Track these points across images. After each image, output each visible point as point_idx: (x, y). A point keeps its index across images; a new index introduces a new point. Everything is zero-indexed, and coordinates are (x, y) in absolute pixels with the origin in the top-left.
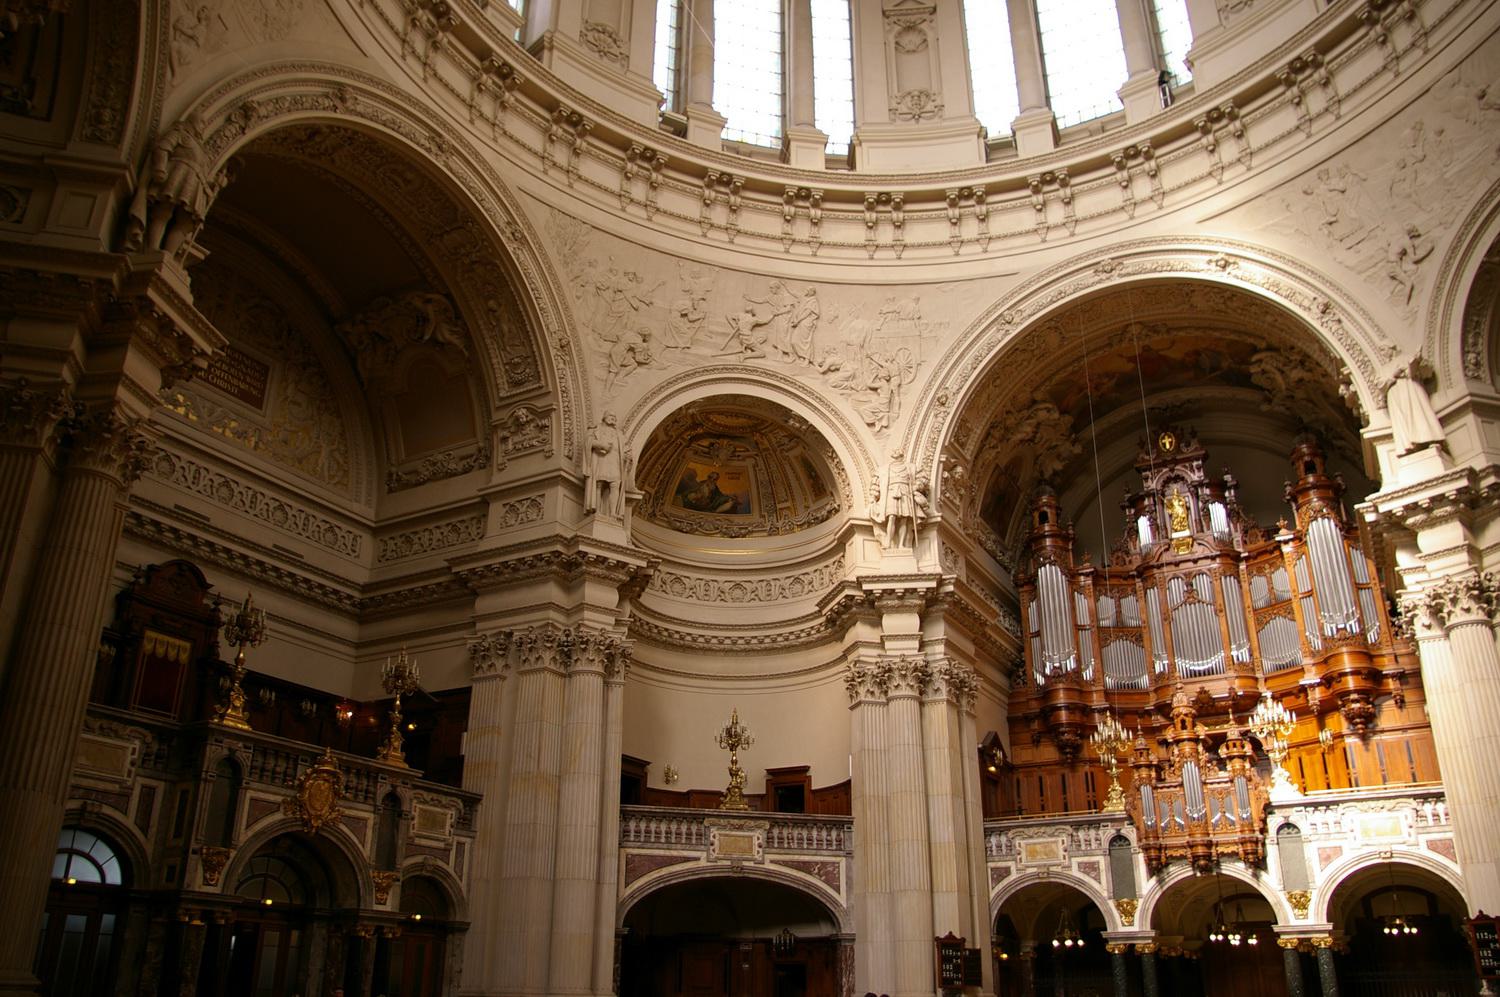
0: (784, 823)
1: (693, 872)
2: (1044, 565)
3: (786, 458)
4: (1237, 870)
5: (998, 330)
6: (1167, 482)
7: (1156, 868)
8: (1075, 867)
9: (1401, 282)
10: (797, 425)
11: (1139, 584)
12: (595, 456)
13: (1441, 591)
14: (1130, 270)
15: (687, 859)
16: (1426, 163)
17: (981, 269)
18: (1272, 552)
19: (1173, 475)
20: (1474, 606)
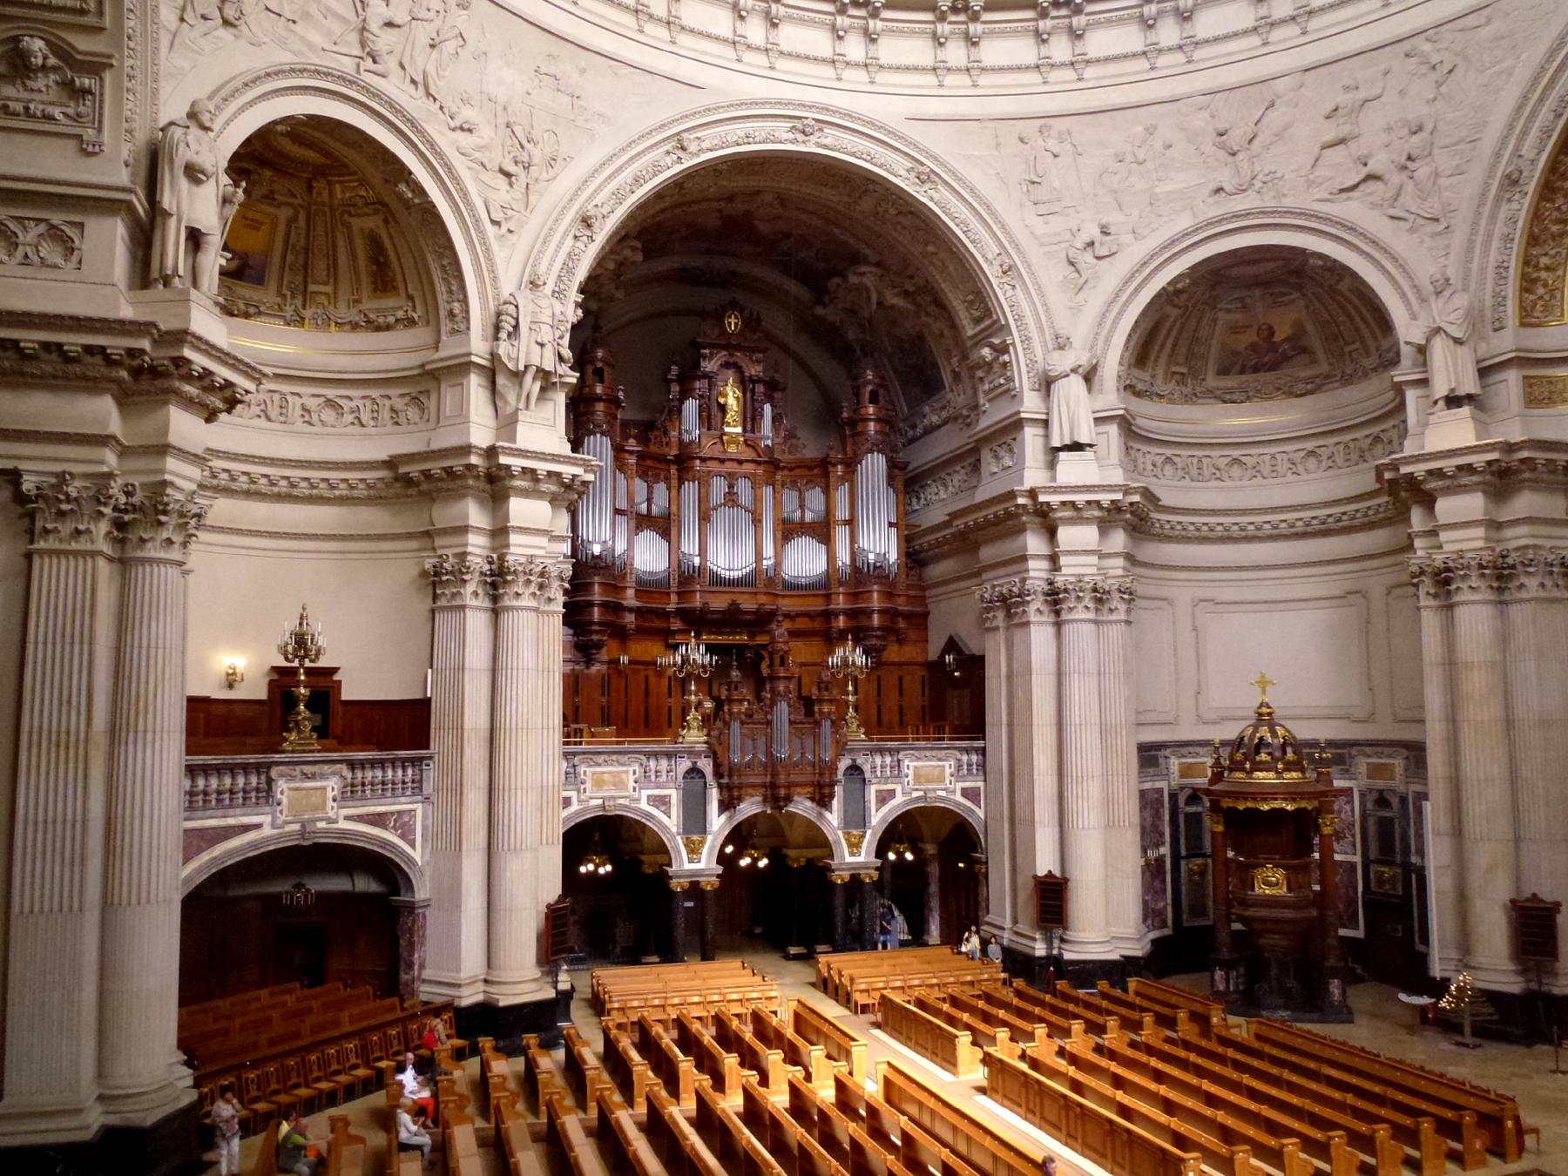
0: (362, 764)
1: (253, 845)
2: (594, 434)
3: (349, 227)
4: (802, 807)
5: (668, 152)
6: (726, 365)
7: (726, 805)
8: (644, 800)
9: (1078, 272)
10: (410, 195)
11: (673, 471)
12: (184, 183)
13: (1070, 587)
14: (828, 141)
15: (247, 828)
16: (1141, 167)
17: (664, 63)
18: (811, 469)
19: (732, 361)
20: (1091, 605)
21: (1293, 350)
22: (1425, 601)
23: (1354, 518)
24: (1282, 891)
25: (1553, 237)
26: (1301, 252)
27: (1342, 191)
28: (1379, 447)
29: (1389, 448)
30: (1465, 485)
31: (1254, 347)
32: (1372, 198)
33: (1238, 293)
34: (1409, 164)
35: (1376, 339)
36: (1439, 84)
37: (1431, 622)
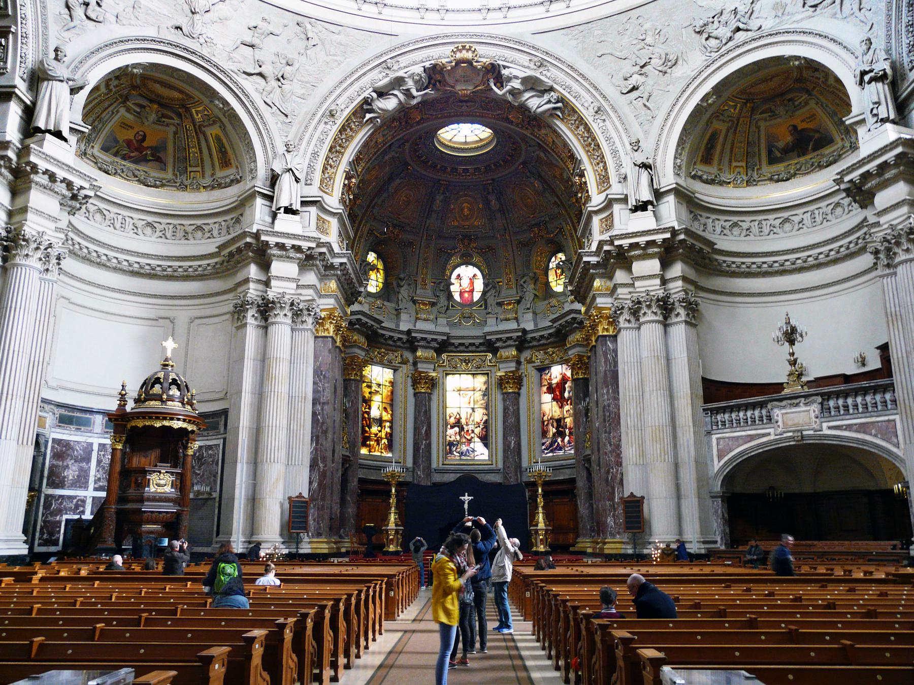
21: (152, 155)
22: (250, 320)
23: (175, 271)
24: (168, 489)
25: (337, 152)
26: (213, 94)
27: (245, 73)
28: (200, 233)
29: (209, 235)
30: (292, 258)
31: (129, 143)
32: (257, 86)
33: (145, 103)
34: (281, 79)
35: (214, 169)
36: (306, 48)
37: (252, 333)
